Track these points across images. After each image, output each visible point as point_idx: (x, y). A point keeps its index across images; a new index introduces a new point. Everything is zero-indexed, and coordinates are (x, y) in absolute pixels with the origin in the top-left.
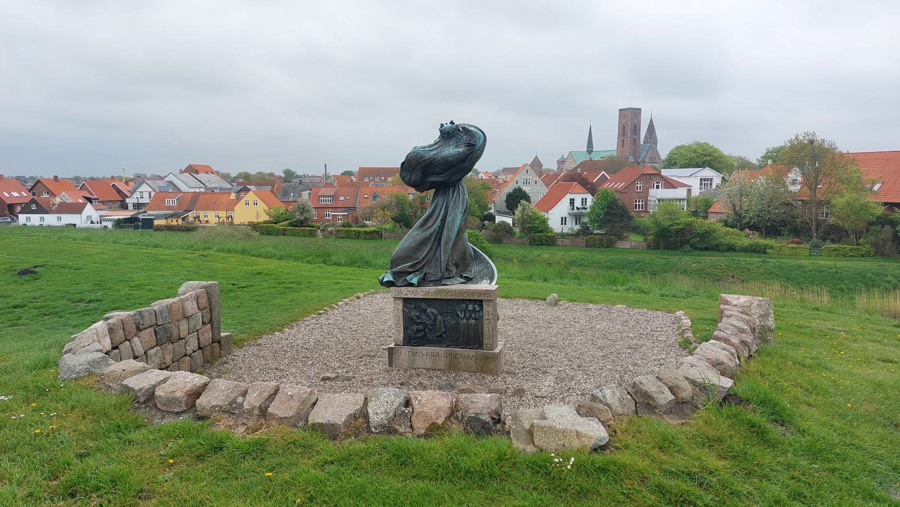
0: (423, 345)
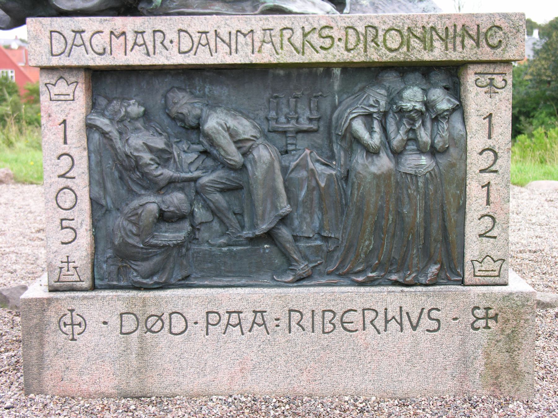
0: (185, 282)
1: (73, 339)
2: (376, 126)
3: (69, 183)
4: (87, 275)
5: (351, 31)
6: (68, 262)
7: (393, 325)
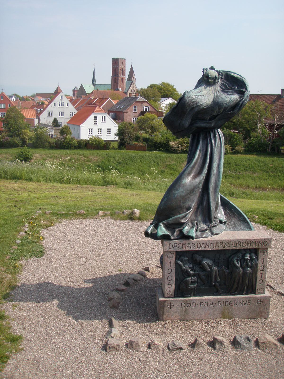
1: (170, 309)
2: (239, 262)
3: (171, 275)
4: (173, 294)
5: (235, 243)
6: (169, 292)
7: (241, 304)
